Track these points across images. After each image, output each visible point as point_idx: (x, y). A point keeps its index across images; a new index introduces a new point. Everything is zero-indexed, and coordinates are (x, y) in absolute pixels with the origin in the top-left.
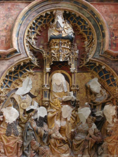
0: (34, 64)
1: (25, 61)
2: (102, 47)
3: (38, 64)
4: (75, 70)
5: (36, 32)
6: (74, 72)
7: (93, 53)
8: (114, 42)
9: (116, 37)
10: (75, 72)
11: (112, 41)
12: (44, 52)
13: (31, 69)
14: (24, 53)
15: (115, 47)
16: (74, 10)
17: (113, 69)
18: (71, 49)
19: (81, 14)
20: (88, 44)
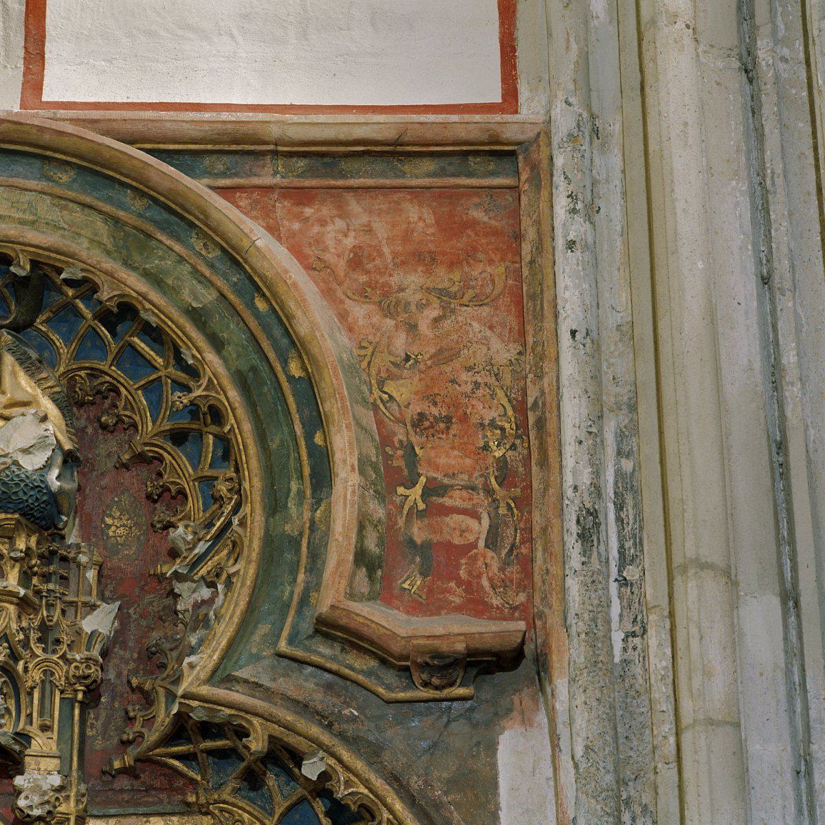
2: (301, 577)
4: (61, 789)
6: (49, 812)
7: (224, 632)
8: (419, 533)
9: (433, 489)
10: (61, 809)
11: (401, 522)
15: (424, 574)
16: (81, 248)
17: (395, 779)
18: (38, 593)
19: (135, 283)
20: (201, 548)
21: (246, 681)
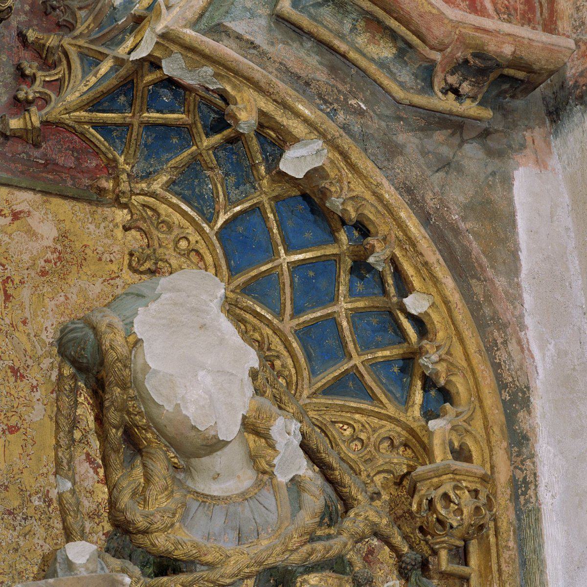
17: (408, 190)
21: (239, 37)
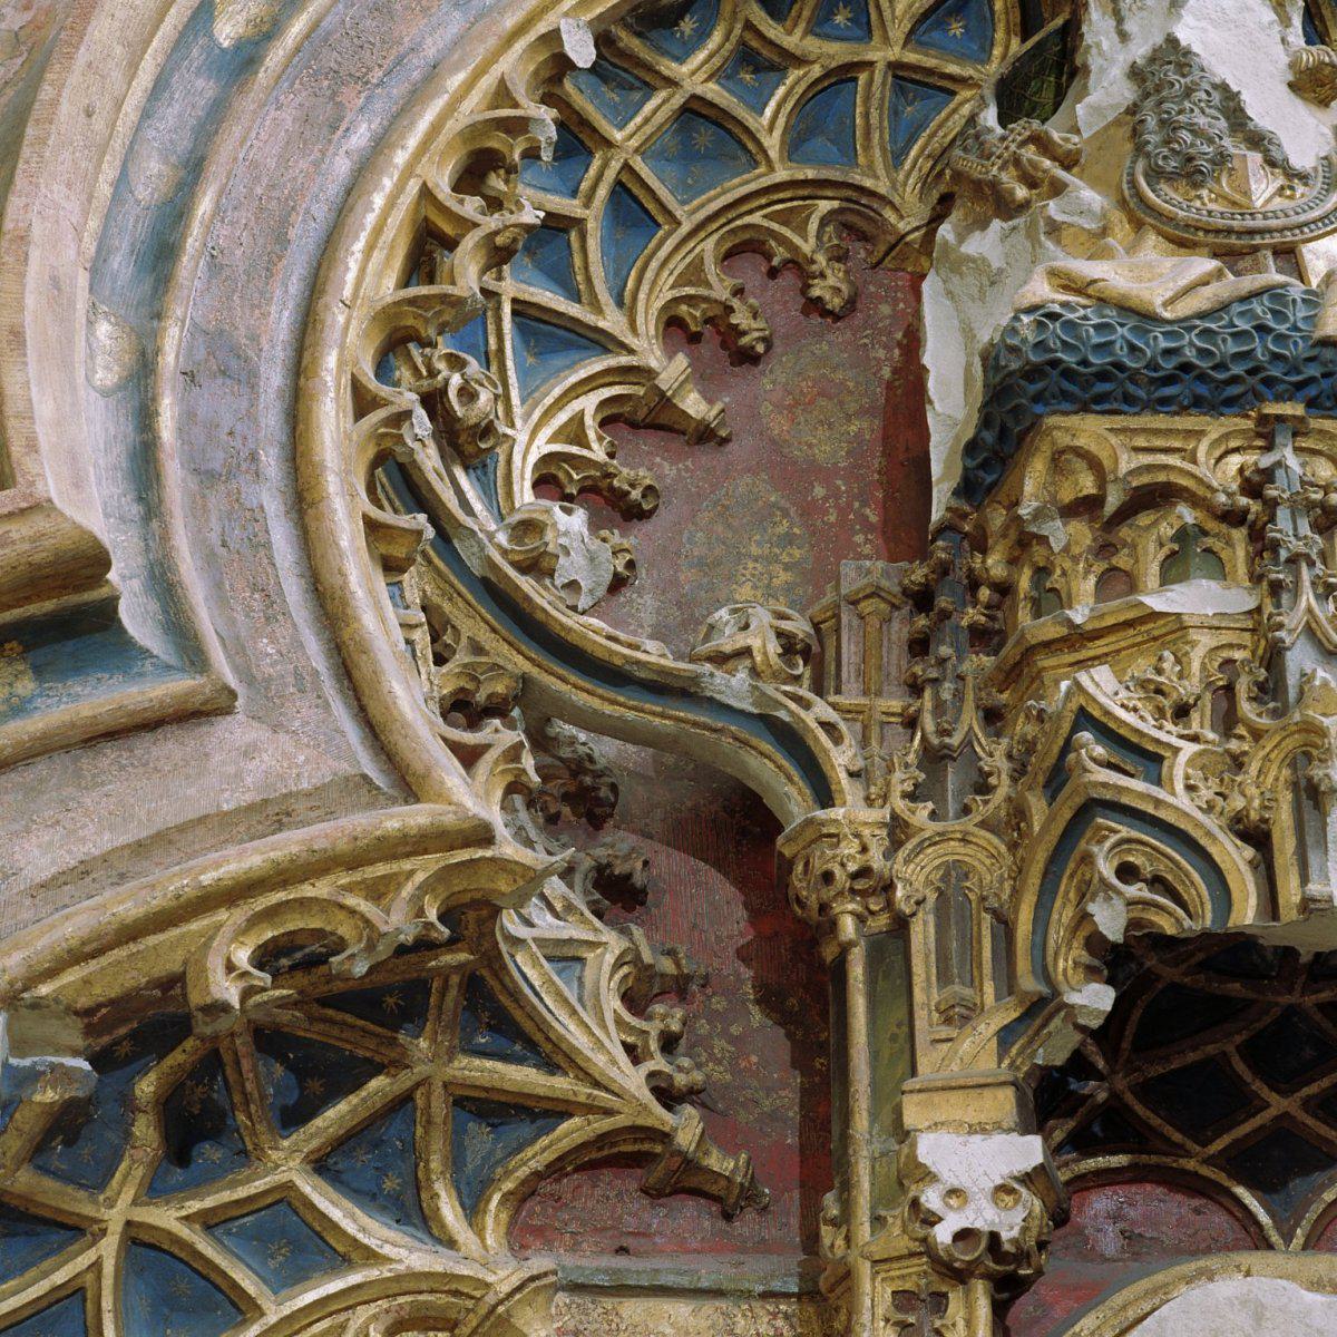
0: (553, 1056)
1: (320, 889)
3: (658, 1063)
5: (602, 342)
12: (840, 759)
13: (473, 1210)
14: (304, 681)
